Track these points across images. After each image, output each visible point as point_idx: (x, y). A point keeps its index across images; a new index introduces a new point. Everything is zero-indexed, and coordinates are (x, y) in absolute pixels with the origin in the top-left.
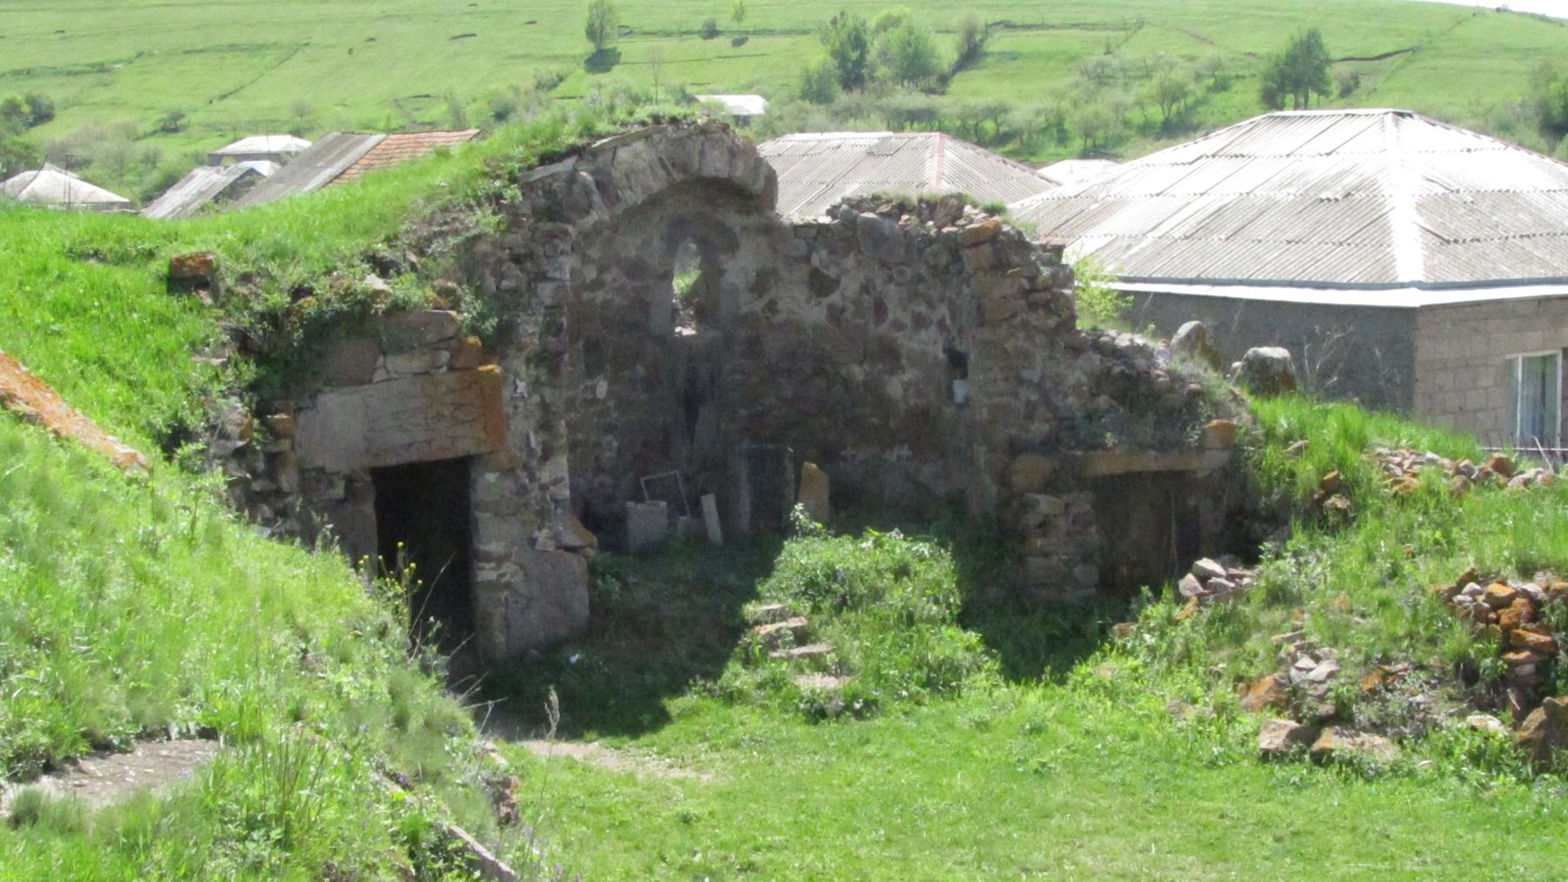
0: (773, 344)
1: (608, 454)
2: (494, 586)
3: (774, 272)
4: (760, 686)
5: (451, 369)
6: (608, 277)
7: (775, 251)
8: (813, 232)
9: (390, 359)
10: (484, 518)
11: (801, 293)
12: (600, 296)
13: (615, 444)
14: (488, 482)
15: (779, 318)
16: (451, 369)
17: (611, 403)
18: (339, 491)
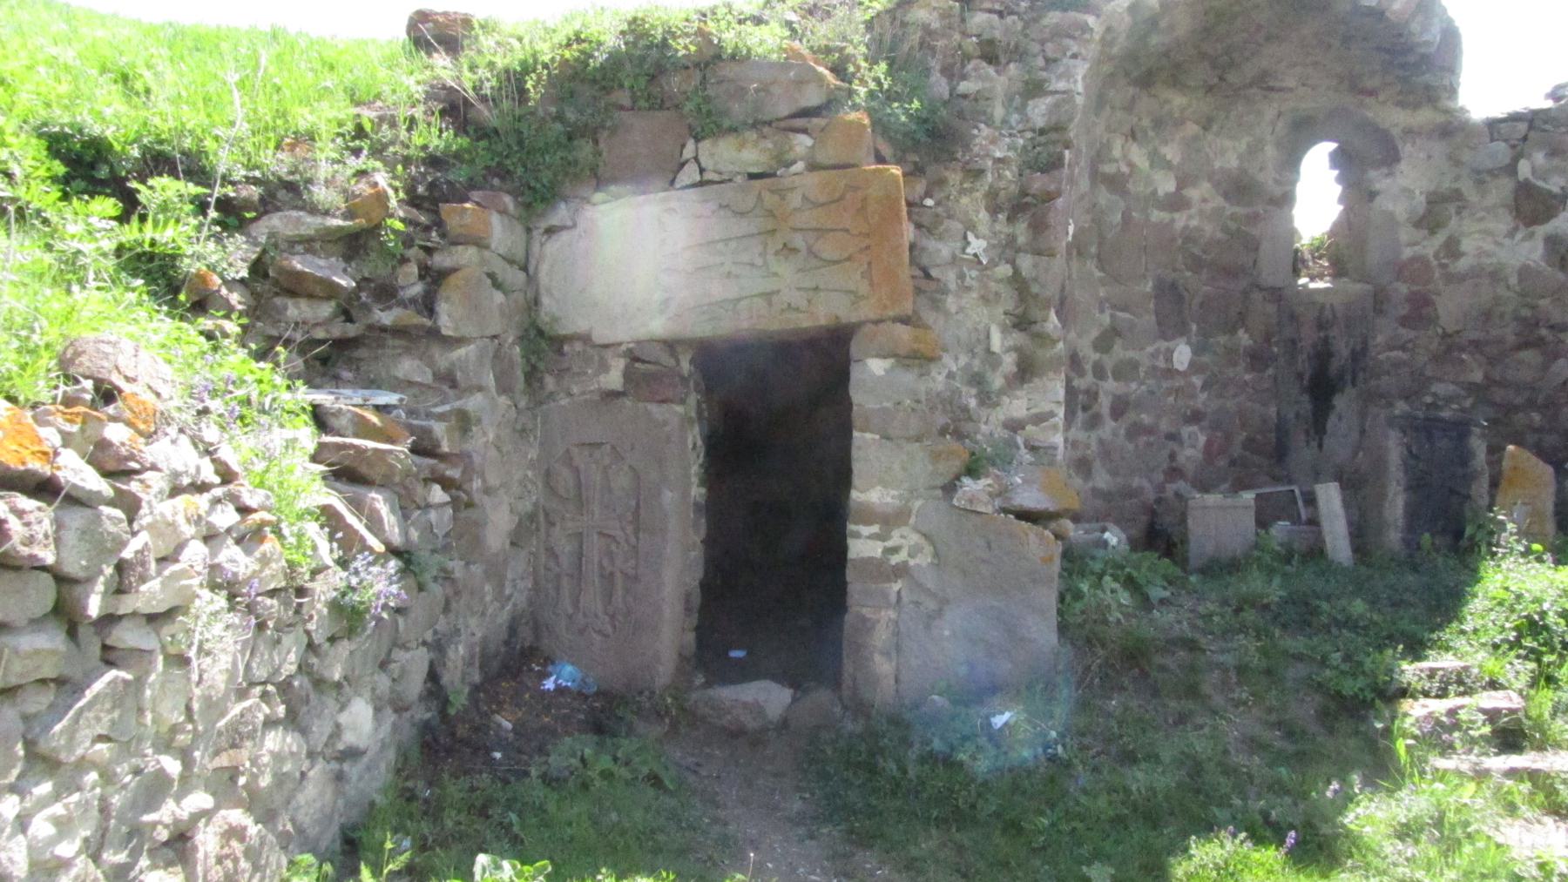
0: (1451, 307)
1: (1189, 452)
2: (882, 571)
3: (1456, 196)
4: (1405, 832)
5: (813, 167)
6: (1193, 194)
7: (1457, 163)
8: (1522, 127)
9: (706, 145)
10: (863, 441)
11: (1502, 223)
12: (1181, 220)
13: (1202, 439)
14: (872, 371)
15: (1463, 264)
16: (813, 167)
17: (1197, 381)
18: (614, 379)
